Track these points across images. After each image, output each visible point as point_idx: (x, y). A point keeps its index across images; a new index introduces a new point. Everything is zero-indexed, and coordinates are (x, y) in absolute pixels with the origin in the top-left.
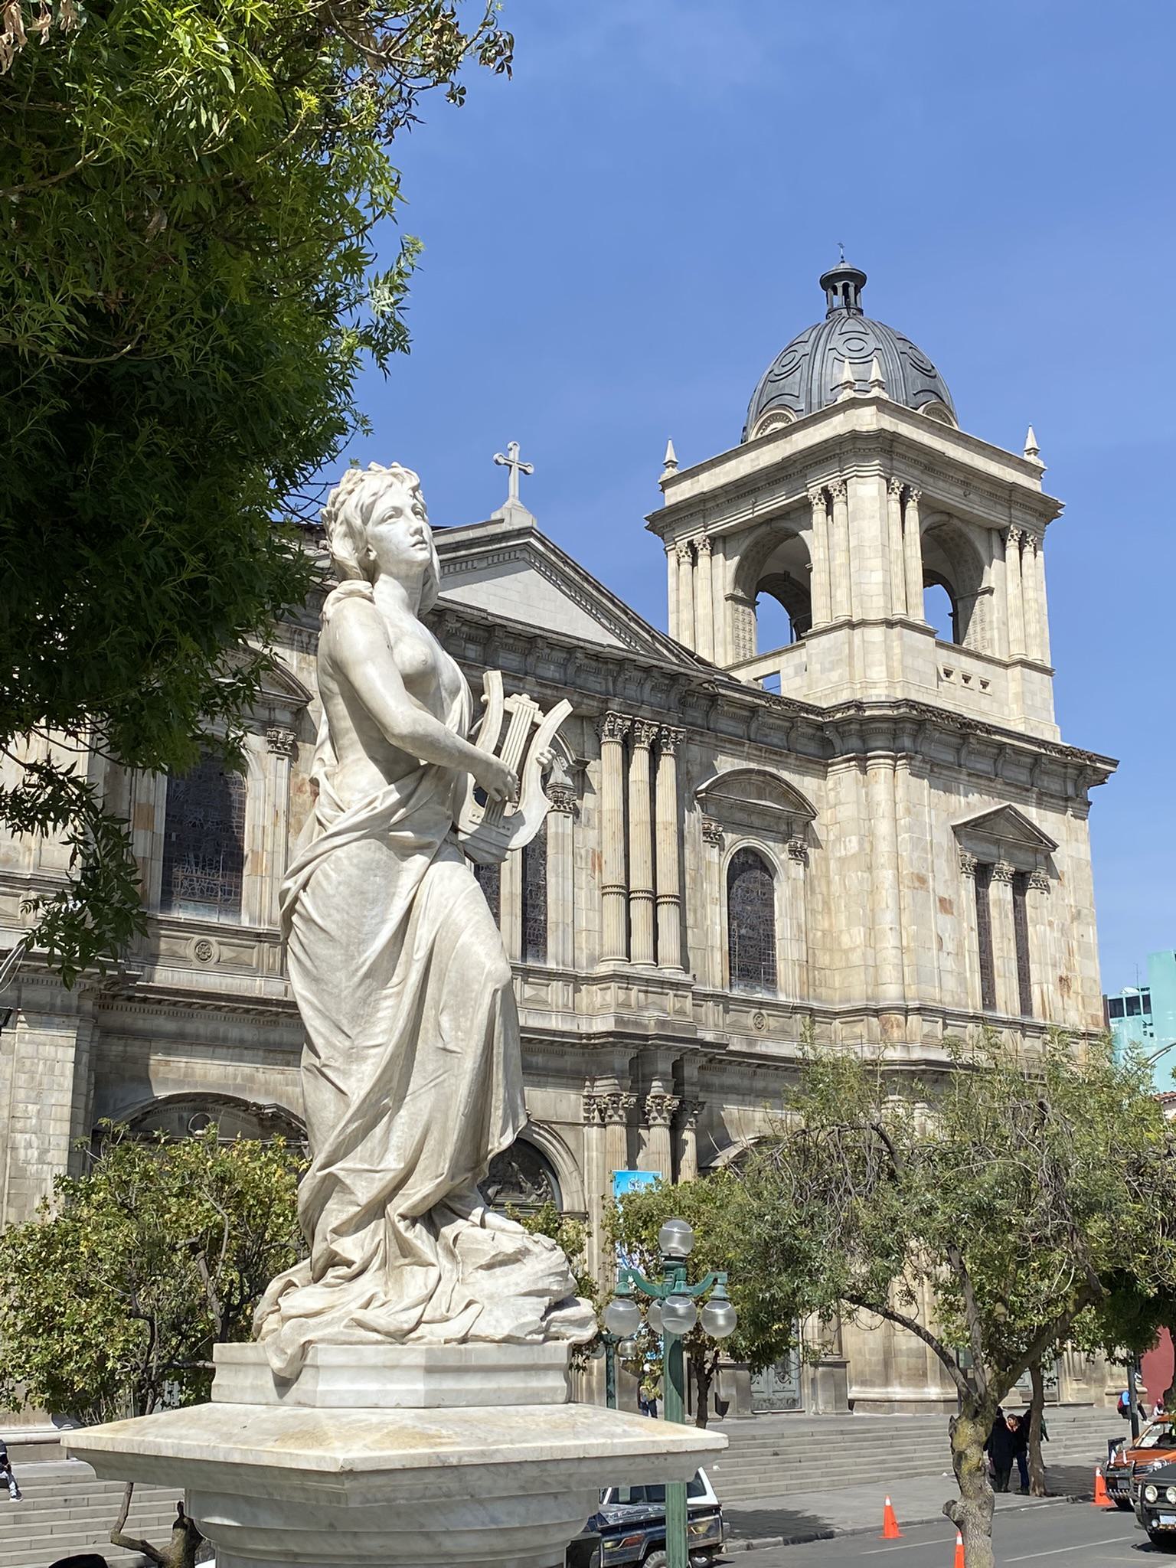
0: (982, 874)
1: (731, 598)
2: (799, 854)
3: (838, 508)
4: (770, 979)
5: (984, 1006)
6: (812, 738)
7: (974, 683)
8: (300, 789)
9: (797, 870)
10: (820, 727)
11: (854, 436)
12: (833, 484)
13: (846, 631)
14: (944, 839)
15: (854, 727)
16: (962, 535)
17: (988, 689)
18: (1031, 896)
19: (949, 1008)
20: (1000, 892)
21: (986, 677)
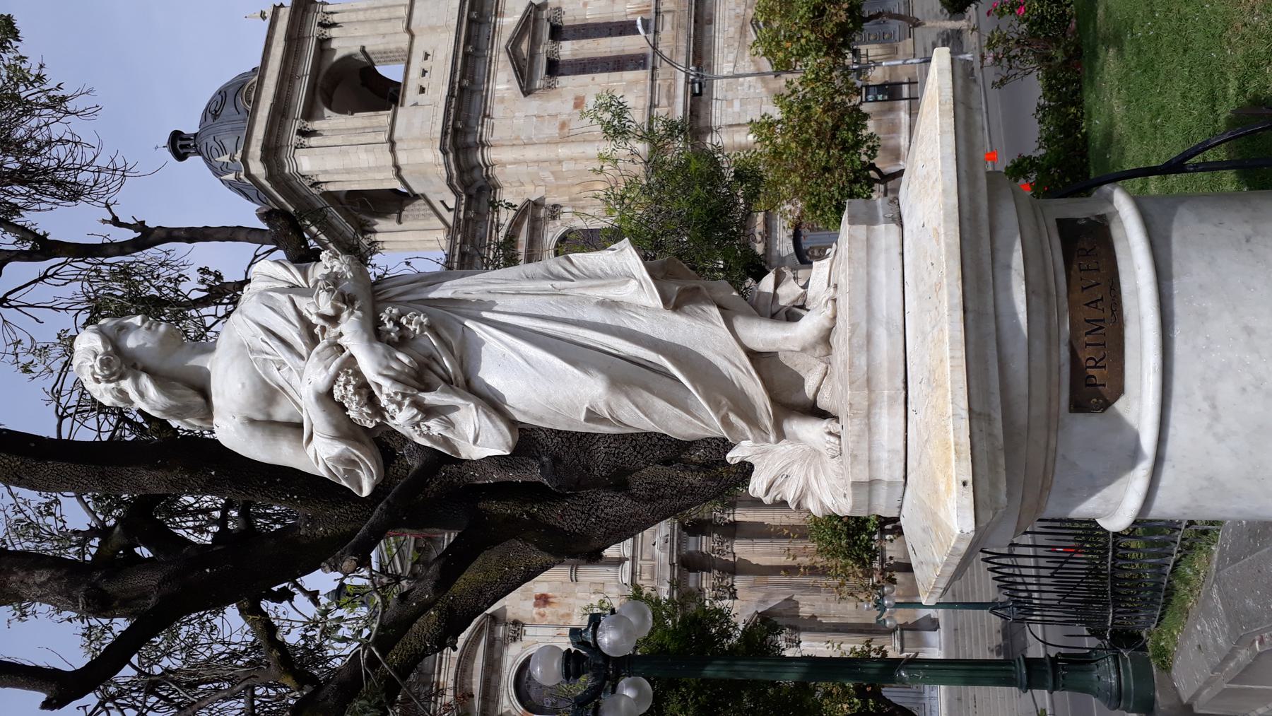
0: (554, 68)
1: (399, 222)
2: (555, 211)
3: (321, 179)
5: (645, 67)
6: (478, 201)
7: (426, 65)
8: (543, 615)
10: (469, 197)
12: (307, 184)
13: (403, 173)
14: (533, 105)
15: (466, 178)
16: (329, 72)
17: (430, 52)
18: (567, 20)
19: (648, 104)
20: (568, 50)
21: (422, 56)
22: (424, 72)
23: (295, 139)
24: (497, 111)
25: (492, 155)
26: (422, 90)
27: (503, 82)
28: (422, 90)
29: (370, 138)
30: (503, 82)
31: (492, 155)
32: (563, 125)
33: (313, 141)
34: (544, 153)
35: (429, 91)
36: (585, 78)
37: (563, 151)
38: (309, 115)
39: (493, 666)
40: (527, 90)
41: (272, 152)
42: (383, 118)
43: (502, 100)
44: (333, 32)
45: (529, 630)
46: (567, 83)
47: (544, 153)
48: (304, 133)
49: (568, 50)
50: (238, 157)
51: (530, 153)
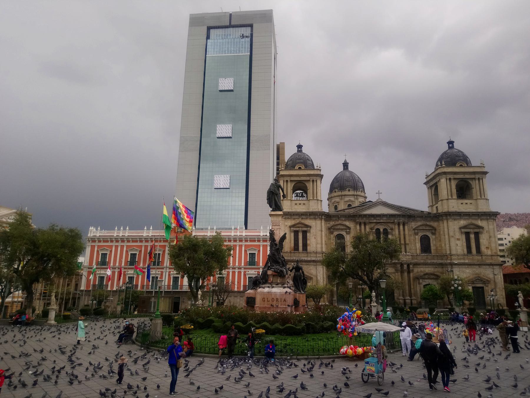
0: (467, 234)
2: (434, 234)
4: (430, 252)
7: (469, 204)
9: (434, 237)
11: (439, 173)
14: (457, 230)
18: (480, 236)
20: (472, 236)
22: (466, 204)
23: (448, 178)
24: (456, 222)
25: (445, 222)
26: (462, 204)
27: (463, 223)
28: (462, 204)
29: (449, 194)
30: (463, 223)
31: (445, 222)
32: (453, 236)
33: (448, 181)
34: (446, 233)
35: (462, 205)
36: (464, 240)
37: (447, 236)
38: (455, 179)
39: (342, 229)
40: (460, 228)
41: (445, 173)
42: (455, 196)
43: (459, 223)
44: (477, 181)
45: (348, 236)
46: (464, 237)
47: (446, 233)
48: (450, 179)
49: (472, 236)
50: (444, 166)
51: (446, 230)
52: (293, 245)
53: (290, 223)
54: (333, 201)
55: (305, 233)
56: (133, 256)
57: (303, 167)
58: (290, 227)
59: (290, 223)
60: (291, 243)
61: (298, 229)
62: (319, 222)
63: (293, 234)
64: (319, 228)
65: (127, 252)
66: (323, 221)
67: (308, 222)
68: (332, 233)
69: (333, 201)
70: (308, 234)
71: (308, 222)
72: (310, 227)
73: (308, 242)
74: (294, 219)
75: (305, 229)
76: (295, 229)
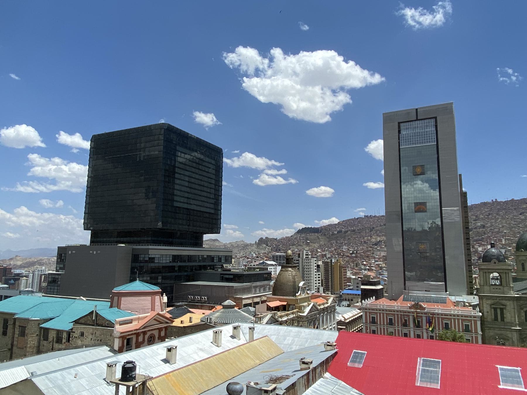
52: (493, 317)
53: (489, 302)
54: (520, 258)
55: (502, 310)
56: (391, 320)
57: (497, 262)
58: (491, 305)
59: (489, 302)
60: (492, 315)
61: (497, 306)
62: (511, 302)
63: (493, 310)
64: (512, 306)
65: (387, 317)
66: (515, 302)
67: (504, 302)
68: (522, 309)
69: (520, 258)
70: (504, 311)
71: (504, 302)
72: (506, 306)
73: (505, 316)
74: (493, 299)
75: (502, 307)
76: (494, 306)
